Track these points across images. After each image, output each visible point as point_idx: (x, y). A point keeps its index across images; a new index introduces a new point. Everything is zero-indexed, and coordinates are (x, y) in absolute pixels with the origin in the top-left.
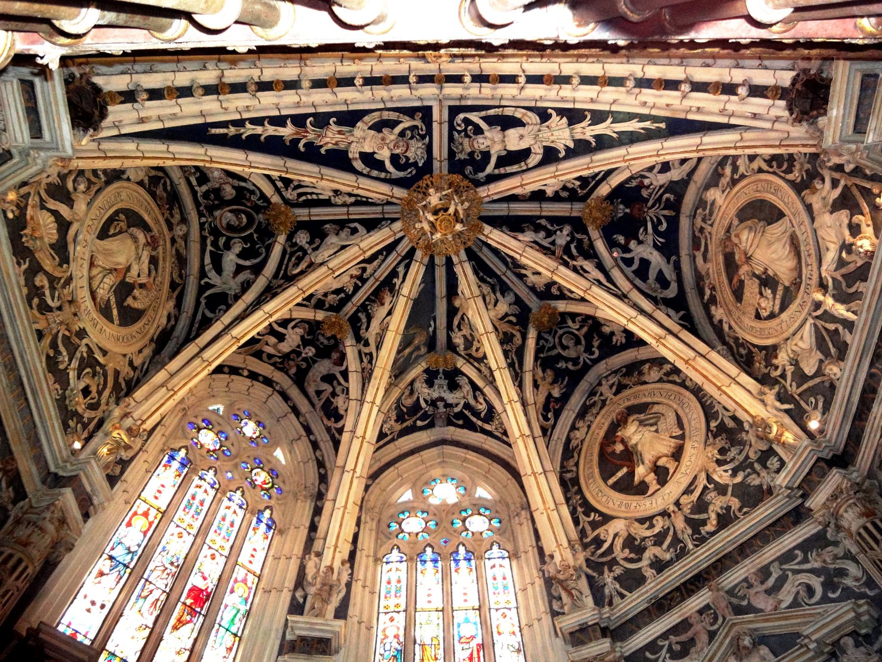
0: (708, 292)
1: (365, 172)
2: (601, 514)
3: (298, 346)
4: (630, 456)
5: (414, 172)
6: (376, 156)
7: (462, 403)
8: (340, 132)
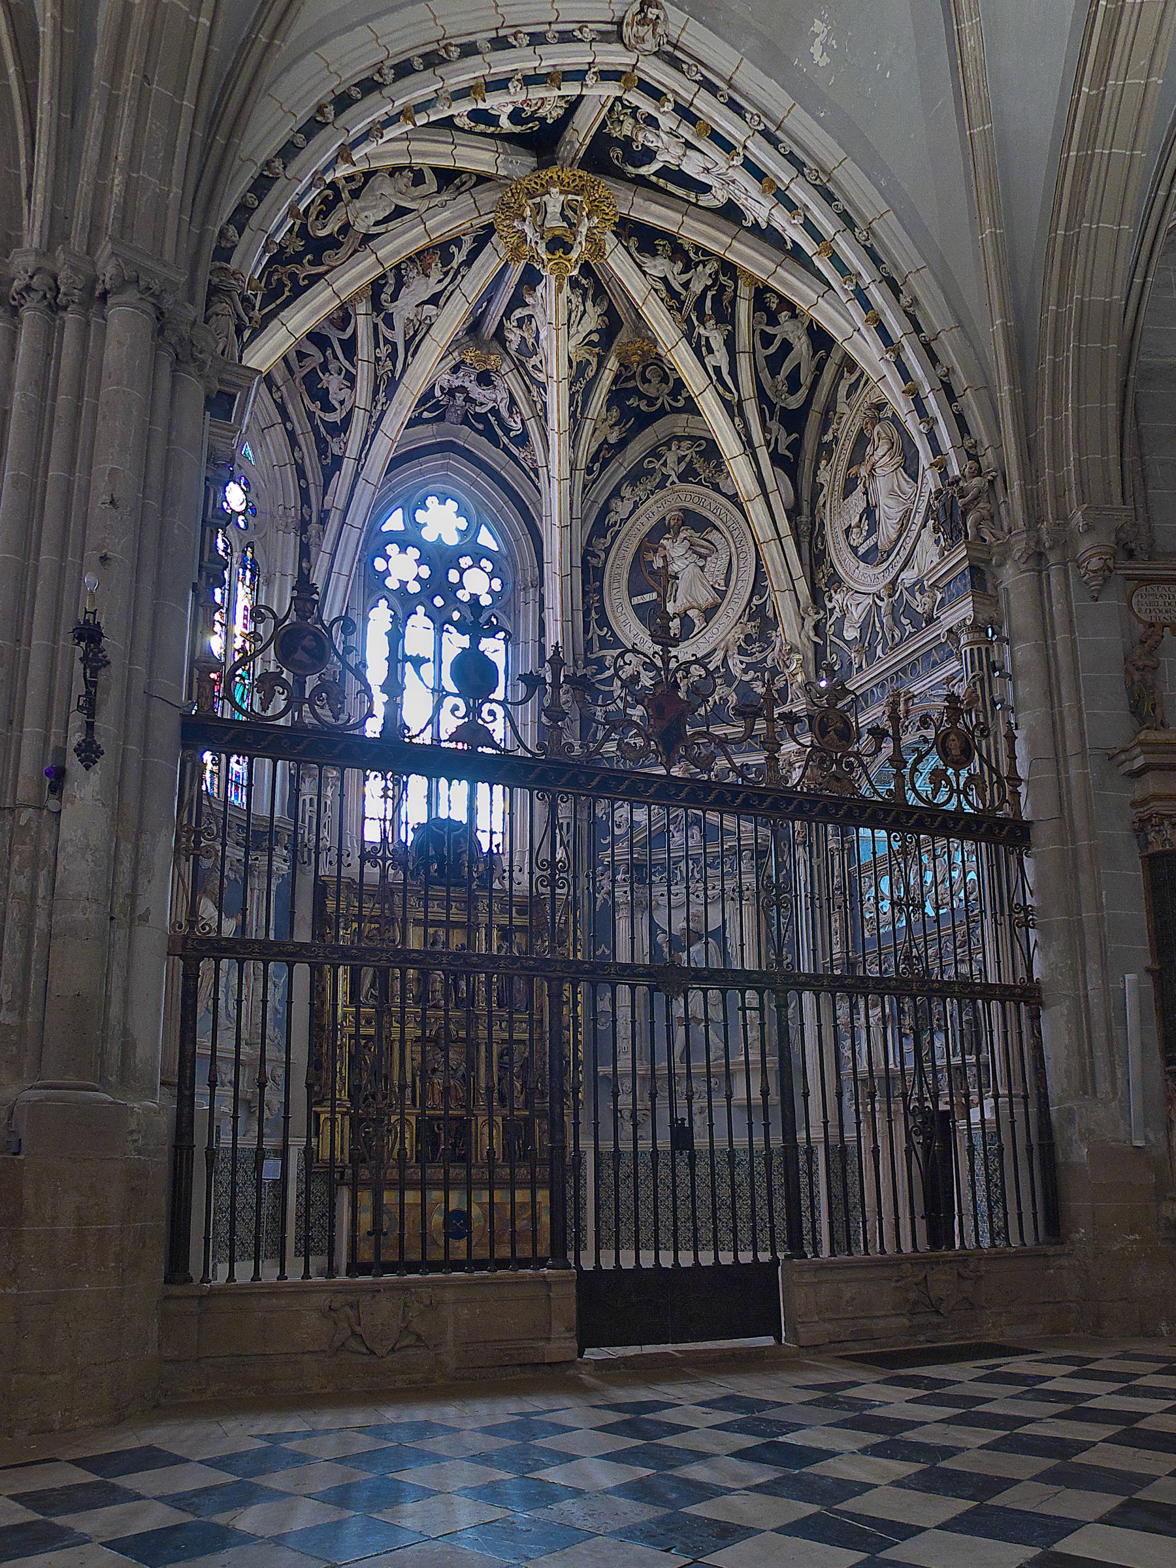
0: (828, 438)
2: (614, 634)
4: (666, 580)
7: (491, 405)
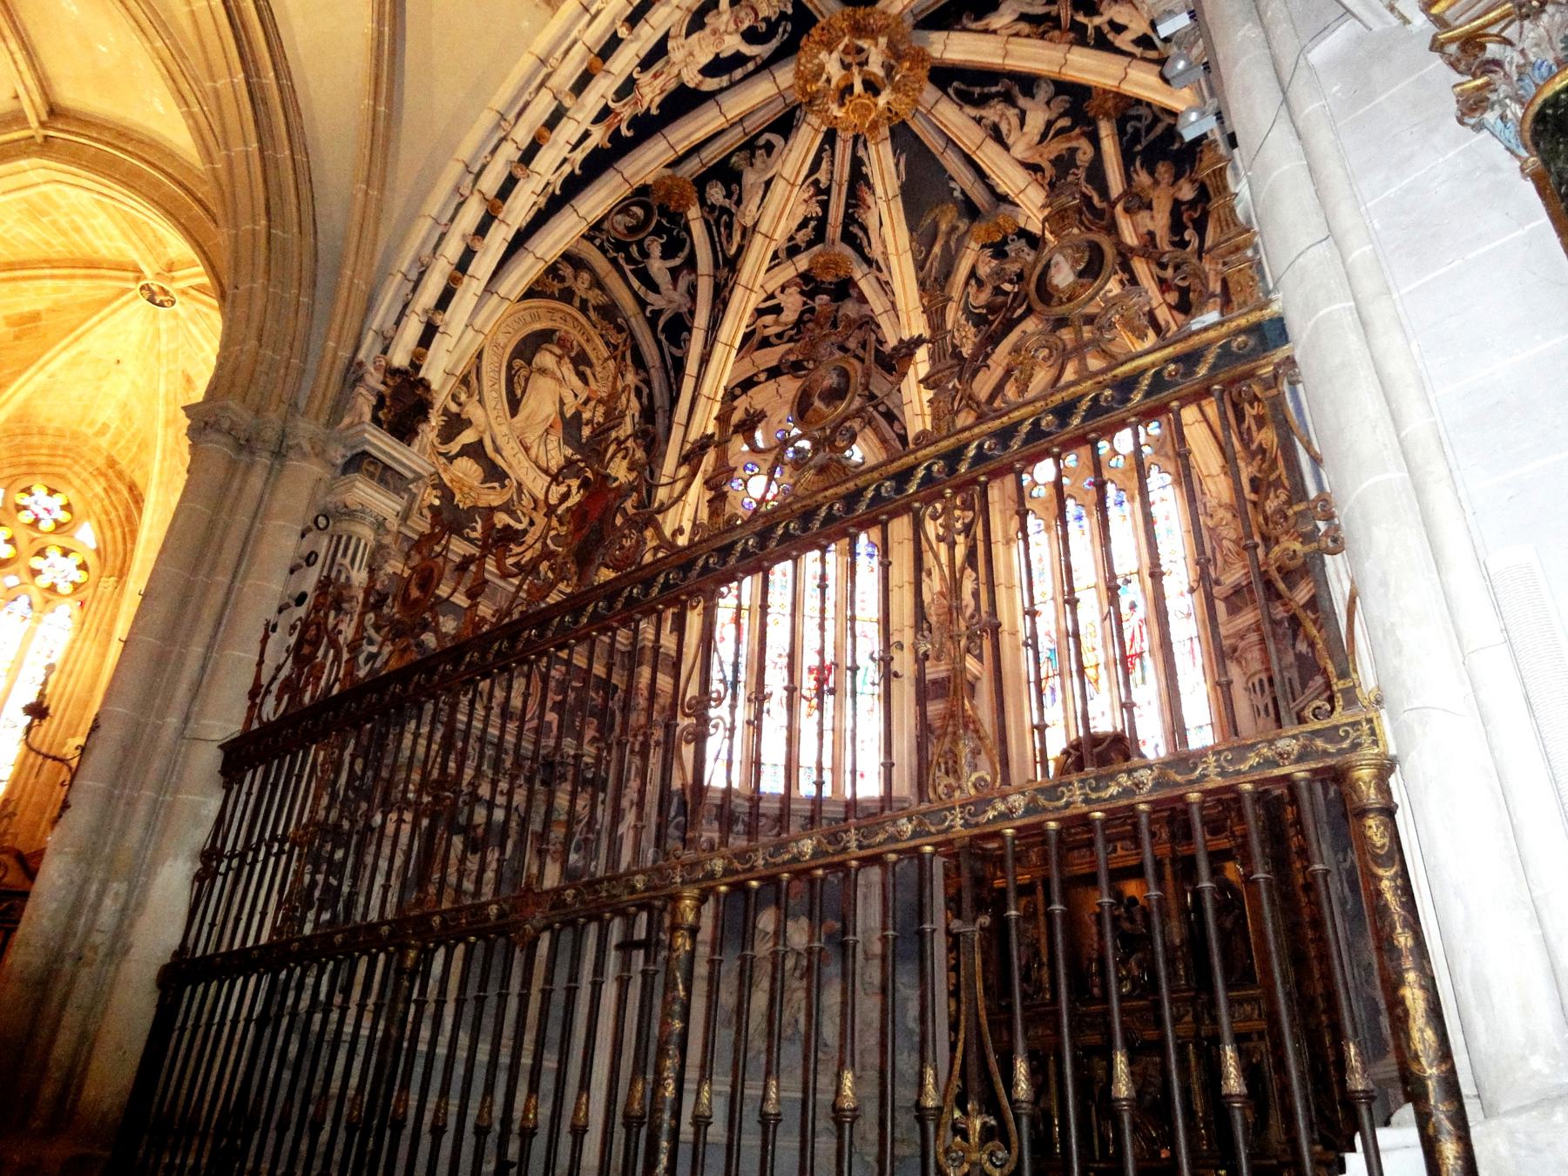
1: (724, 84)
3: (805, 303)
5: (789, 28)
6: (723, 55)
8: (655, 76)
